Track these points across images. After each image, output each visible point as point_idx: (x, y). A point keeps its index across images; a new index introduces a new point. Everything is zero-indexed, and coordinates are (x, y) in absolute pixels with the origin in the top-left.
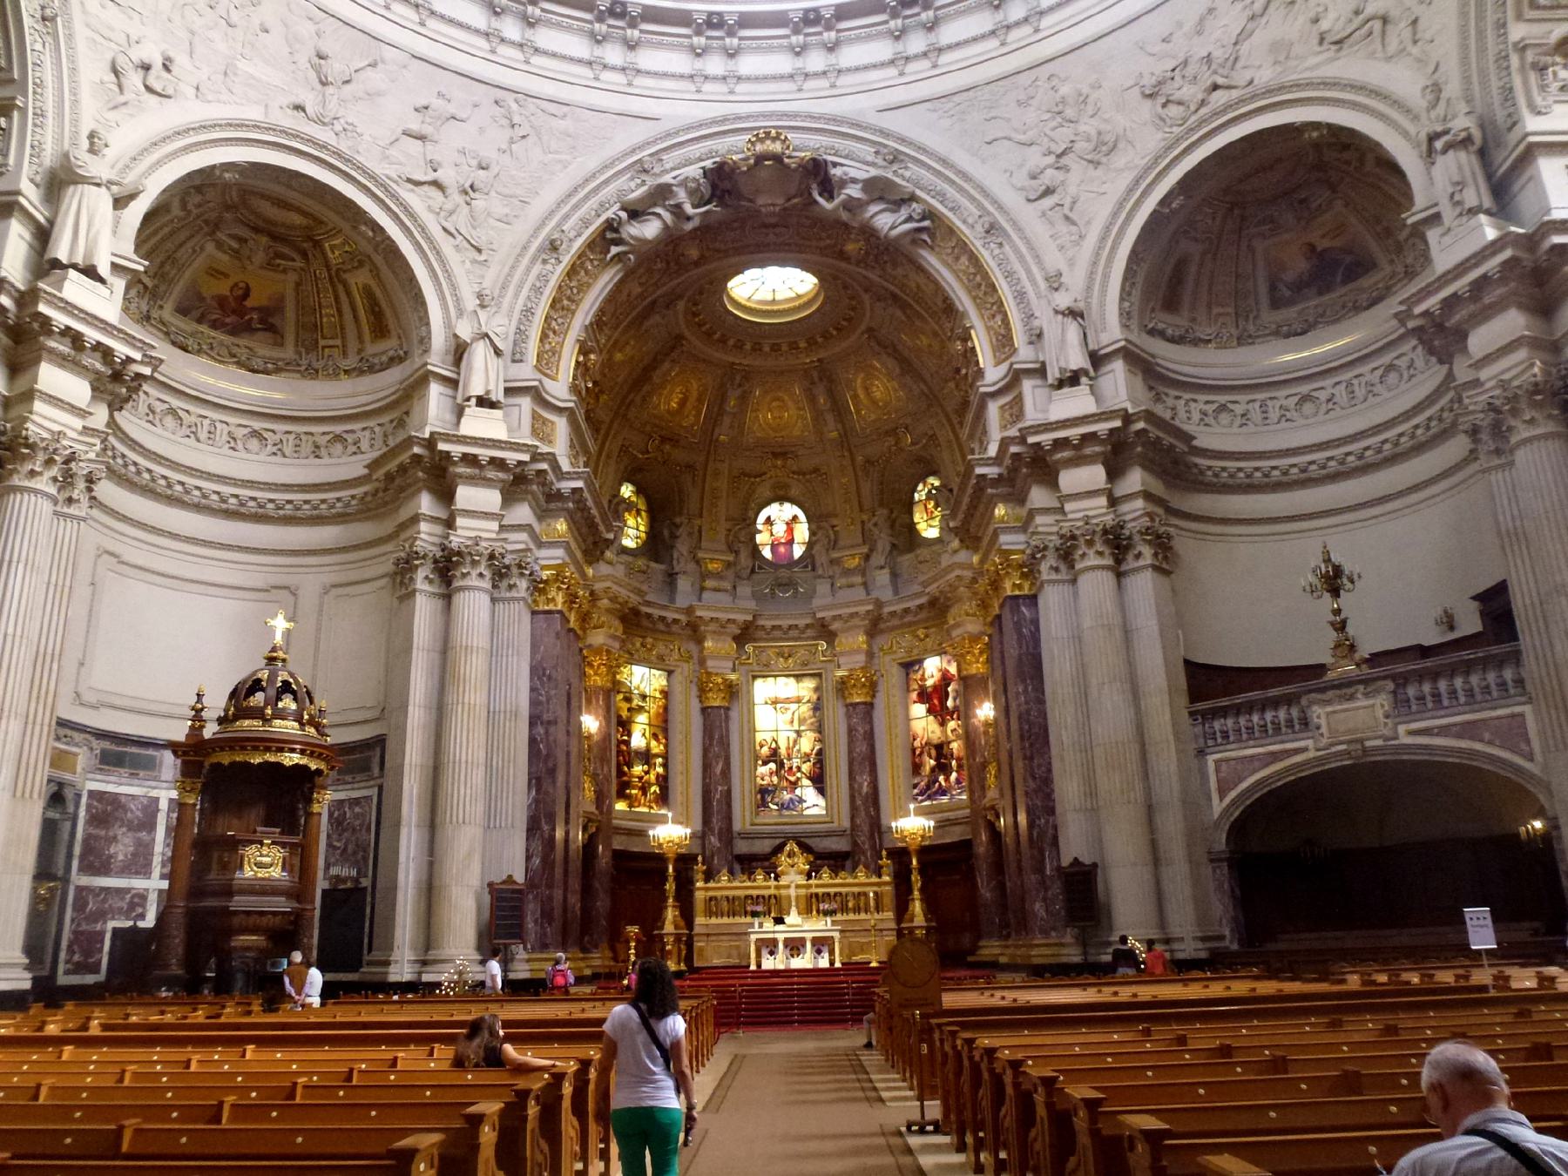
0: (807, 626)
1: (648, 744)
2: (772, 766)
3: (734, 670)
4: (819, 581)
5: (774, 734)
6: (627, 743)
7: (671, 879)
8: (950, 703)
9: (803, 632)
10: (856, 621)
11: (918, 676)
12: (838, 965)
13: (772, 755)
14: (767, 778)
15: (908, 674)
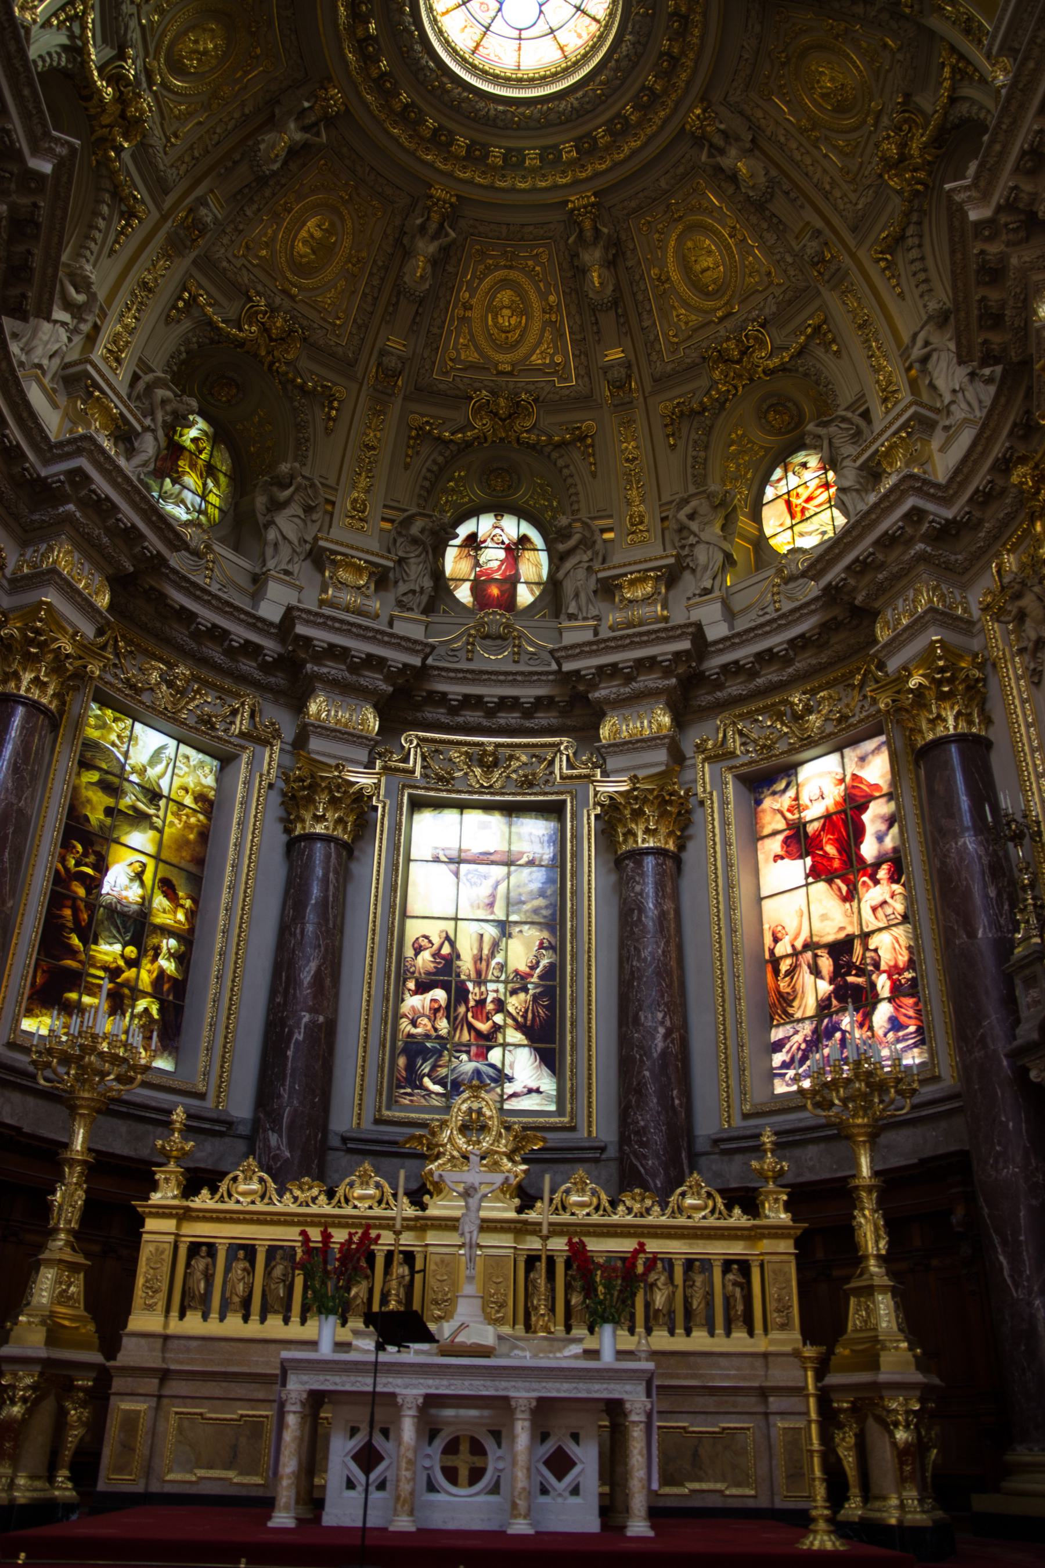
0: (540, 703)
1: (146, 902)
2: (440, 995)
3: (370, 765)
4: (566, 624)
5: (449, 926)
6: (94, 884)
7: (73, 1176)
8: (869, 849)
9: (528, 714)
10: (649, 681)
11: (785, 801)
12: (639, 1527)
13: (438, 972)
14: (425, 1021)
15: (759, 802)
